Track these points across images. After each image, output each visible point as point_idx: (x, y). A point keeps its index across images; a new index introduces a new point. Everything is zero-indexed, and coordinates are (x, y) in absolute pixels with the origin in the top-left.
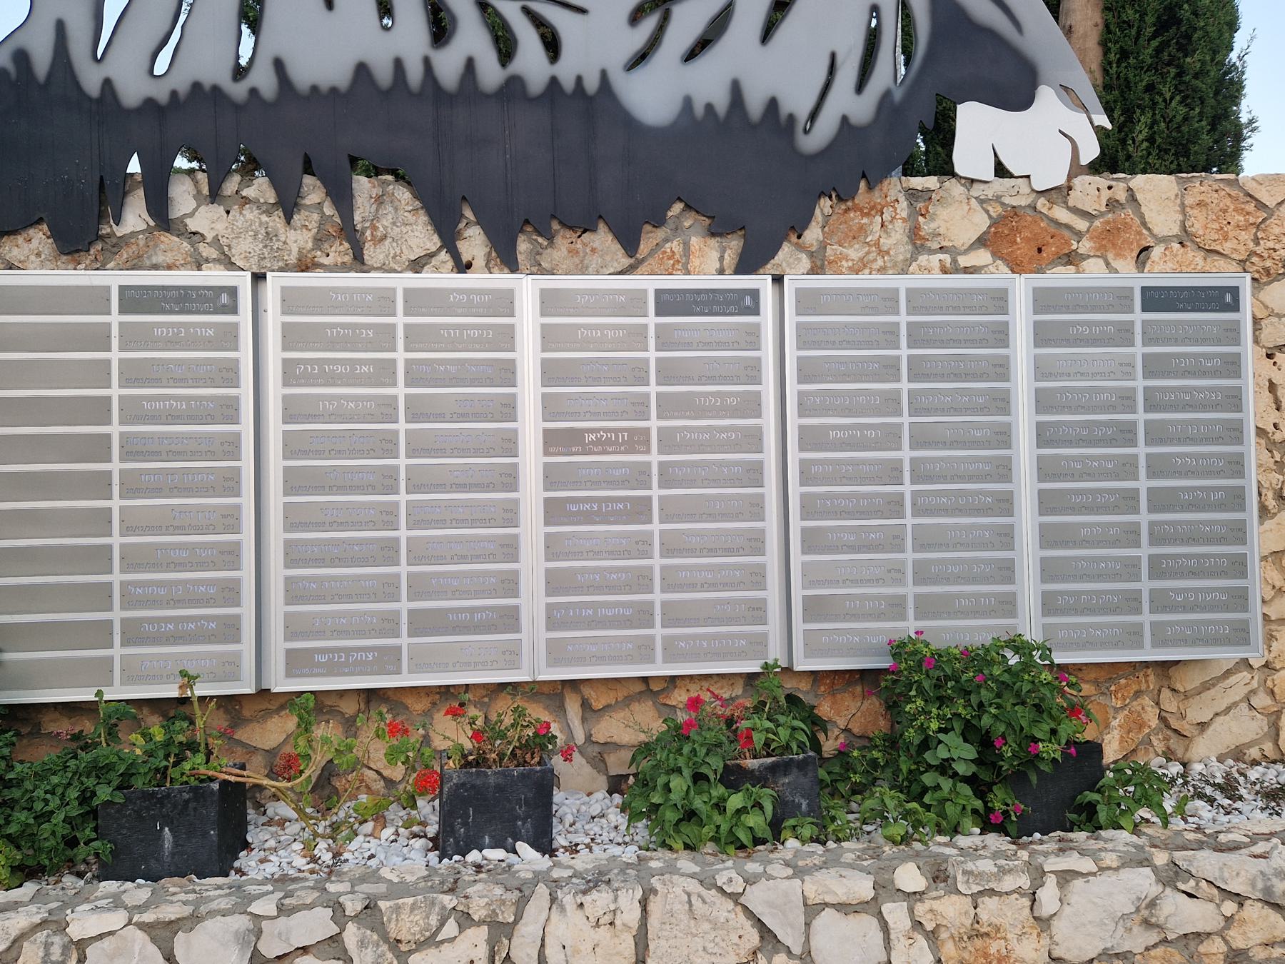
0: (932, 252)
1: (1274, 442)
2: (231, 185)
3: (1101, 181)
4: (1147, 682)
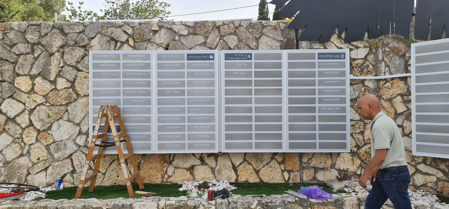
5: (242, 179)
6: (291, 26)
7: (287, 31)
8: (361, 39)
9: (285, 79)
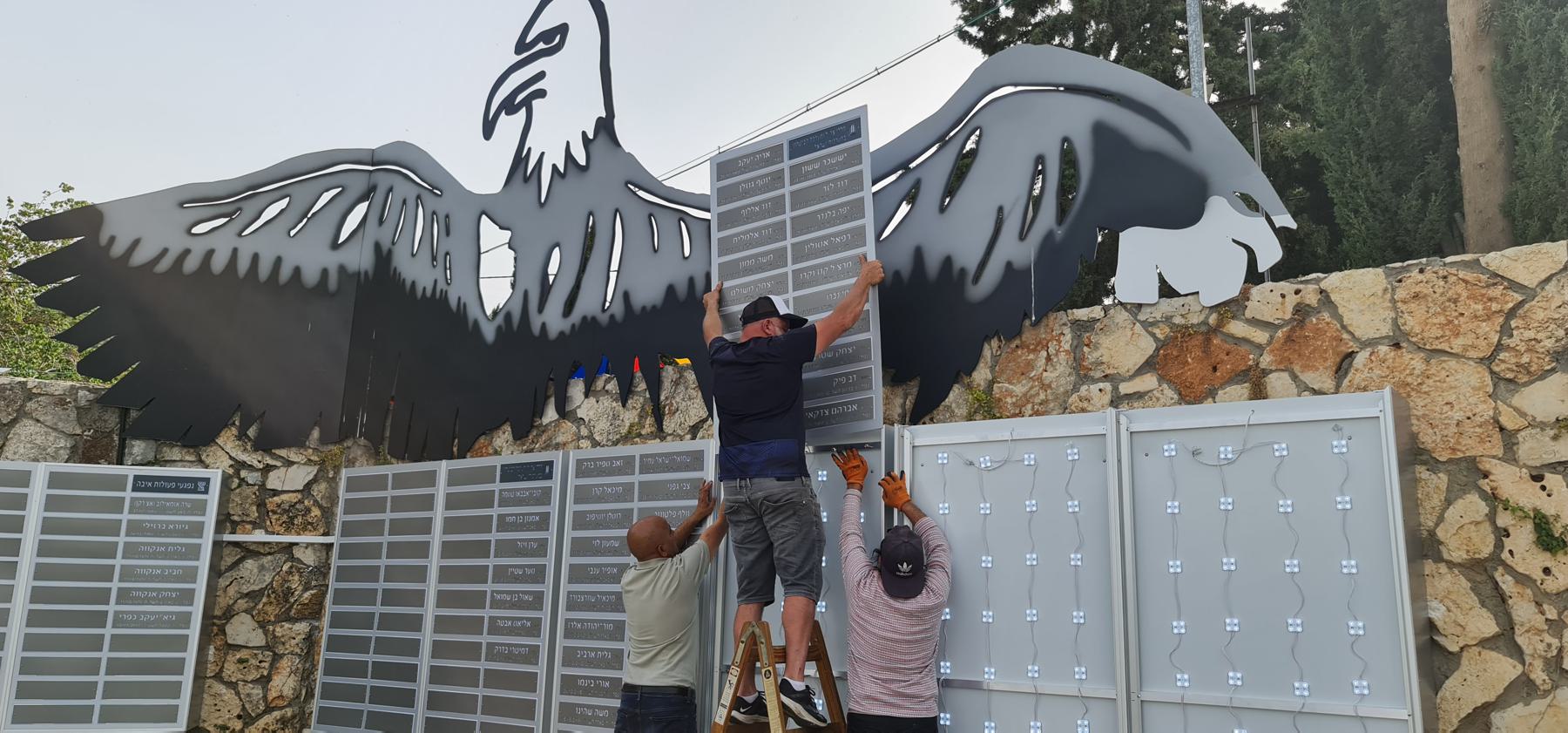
0: (1095, 381)
1: (1546, 594)
2: (600, 384)
3: (1286, 286)
6: (104, 400)
7: (96, 412)
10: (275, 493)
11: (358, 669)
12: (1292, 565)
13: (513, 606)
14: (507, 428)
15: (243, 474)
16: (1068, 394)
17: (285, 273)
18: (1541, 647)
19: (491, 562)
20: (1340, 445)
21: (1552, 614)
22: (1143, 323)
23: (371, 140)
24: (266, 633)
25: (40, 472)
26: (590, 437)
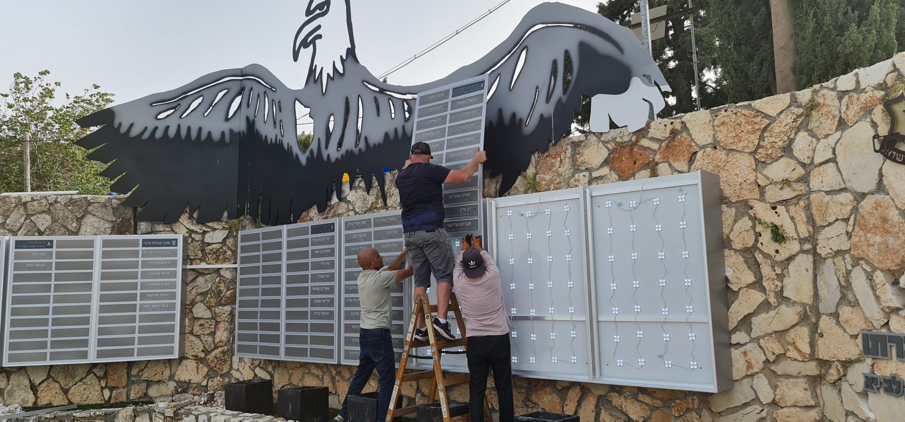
0: (582, 171)
2: (357, 183)
3: (667, 121)
4: (693, 403)
5: (43, 401)
6: (125, 203)
7: (122, 209)
8: (218, 219)
9: (97, 271)
10: (209, 244)
11: (253, 326)
12: (661, 255)
13: (321, 293)
14: (315, 207)
15: (193, 236)
16: (569, 178)
17: (204, 135)
18: (773, 286)
19: (310, 272)
20: (681, 198)
21: (779, 271)
22: (602, 142)
23: (241, 64)
24: (211, 311)
25: (98, 240)
26: (354, 210)
